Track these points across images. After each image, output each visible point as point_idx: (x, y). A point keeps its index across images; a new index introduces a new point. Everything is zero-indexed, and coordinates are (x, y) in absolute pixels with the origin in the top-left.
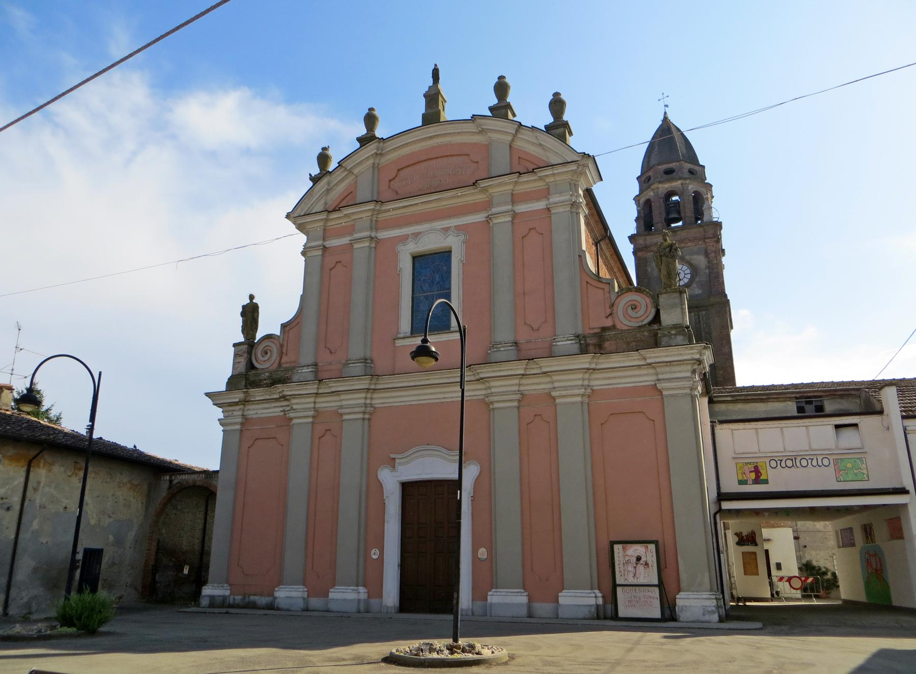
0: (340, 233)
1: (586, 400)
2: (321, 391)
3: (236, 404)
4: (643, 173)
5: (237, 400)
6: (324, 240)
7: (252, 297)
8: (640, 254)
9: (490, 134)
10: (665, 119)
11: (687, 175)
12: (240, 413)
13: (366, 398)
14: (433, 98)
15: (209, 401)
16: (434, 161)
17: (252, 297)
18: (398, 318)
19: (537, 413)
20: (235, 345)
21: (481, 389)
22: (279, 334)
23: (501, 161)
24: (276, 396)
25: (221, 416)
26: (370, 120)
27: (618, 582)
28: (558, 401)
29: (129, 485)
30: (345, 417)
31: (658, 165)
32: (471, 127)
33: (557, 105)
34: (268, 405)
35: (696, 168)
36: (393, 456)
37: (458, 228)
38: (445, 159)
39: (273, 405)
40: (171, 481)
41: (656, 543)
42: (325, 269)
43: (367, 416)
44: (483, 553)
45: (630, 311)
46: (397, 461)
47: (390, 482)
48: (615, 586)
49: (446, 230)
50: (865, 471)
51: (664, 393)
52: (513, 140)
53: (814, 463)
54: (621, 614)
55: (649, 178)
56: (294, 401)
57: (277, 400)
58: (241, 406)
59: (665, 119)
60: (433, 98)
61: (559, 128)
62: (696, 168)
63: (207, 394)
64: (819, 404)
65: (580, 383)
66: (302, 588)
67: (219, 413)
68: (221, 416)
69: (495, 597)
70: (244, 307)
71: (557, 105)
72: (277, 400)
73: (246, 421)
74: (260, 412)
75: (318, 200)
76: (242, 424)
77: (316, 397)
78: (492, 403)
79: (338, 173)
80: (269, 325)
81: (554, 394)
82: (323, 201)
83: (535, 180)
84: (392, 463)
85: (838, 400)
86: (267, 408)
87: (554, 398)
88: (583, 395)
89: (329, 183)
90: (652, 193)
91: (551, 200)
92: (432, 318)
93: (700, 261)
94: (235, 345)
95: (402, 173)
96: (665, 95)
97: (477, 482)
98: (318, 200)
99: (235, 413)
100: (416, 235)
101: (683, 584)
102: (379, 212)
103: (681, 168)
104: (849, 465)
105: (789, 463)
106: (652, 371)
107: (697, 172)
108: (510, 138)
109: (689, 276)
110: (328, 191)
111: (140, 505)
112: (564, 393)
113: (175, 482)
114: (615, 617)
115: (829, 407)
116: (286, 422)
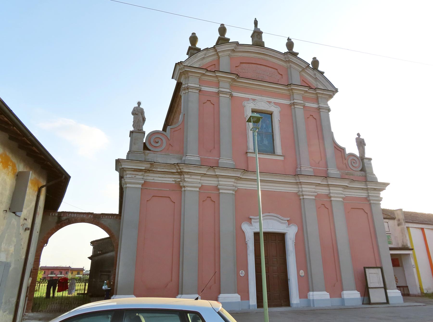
0: (210, 84)
2: (208, 173)
3: (141, 170)
5: (144, 168)
7: (139, 104)
9: (291, 64)
17: (139, 104)
18: (246, 142)
19: (325, 204)
21: (295, 188)
26: (222, 30)
30: (221, 191)
32: (282, 57)
34: (163, 176)
36: (251, 217)
37: (275, 103)
39: (167, 176)
43: (234, 193)
44: (302, 273)
46: (253, 220)
49: (270, 102)
56: (186, 176)
57: (173, 173)
72: (173, 173)
74: (155, 178)
75: (197, 61)
76: (143, 185)
78: (303, 195)
79: (211, 51)
83: (313, 93)
84: (249, 220)
86: (163, 177)
99: (137, 177)
100: (254, 100)
106: (366, 192)
112: (336, 195)
114: (369, 303)
116: (179, 187)
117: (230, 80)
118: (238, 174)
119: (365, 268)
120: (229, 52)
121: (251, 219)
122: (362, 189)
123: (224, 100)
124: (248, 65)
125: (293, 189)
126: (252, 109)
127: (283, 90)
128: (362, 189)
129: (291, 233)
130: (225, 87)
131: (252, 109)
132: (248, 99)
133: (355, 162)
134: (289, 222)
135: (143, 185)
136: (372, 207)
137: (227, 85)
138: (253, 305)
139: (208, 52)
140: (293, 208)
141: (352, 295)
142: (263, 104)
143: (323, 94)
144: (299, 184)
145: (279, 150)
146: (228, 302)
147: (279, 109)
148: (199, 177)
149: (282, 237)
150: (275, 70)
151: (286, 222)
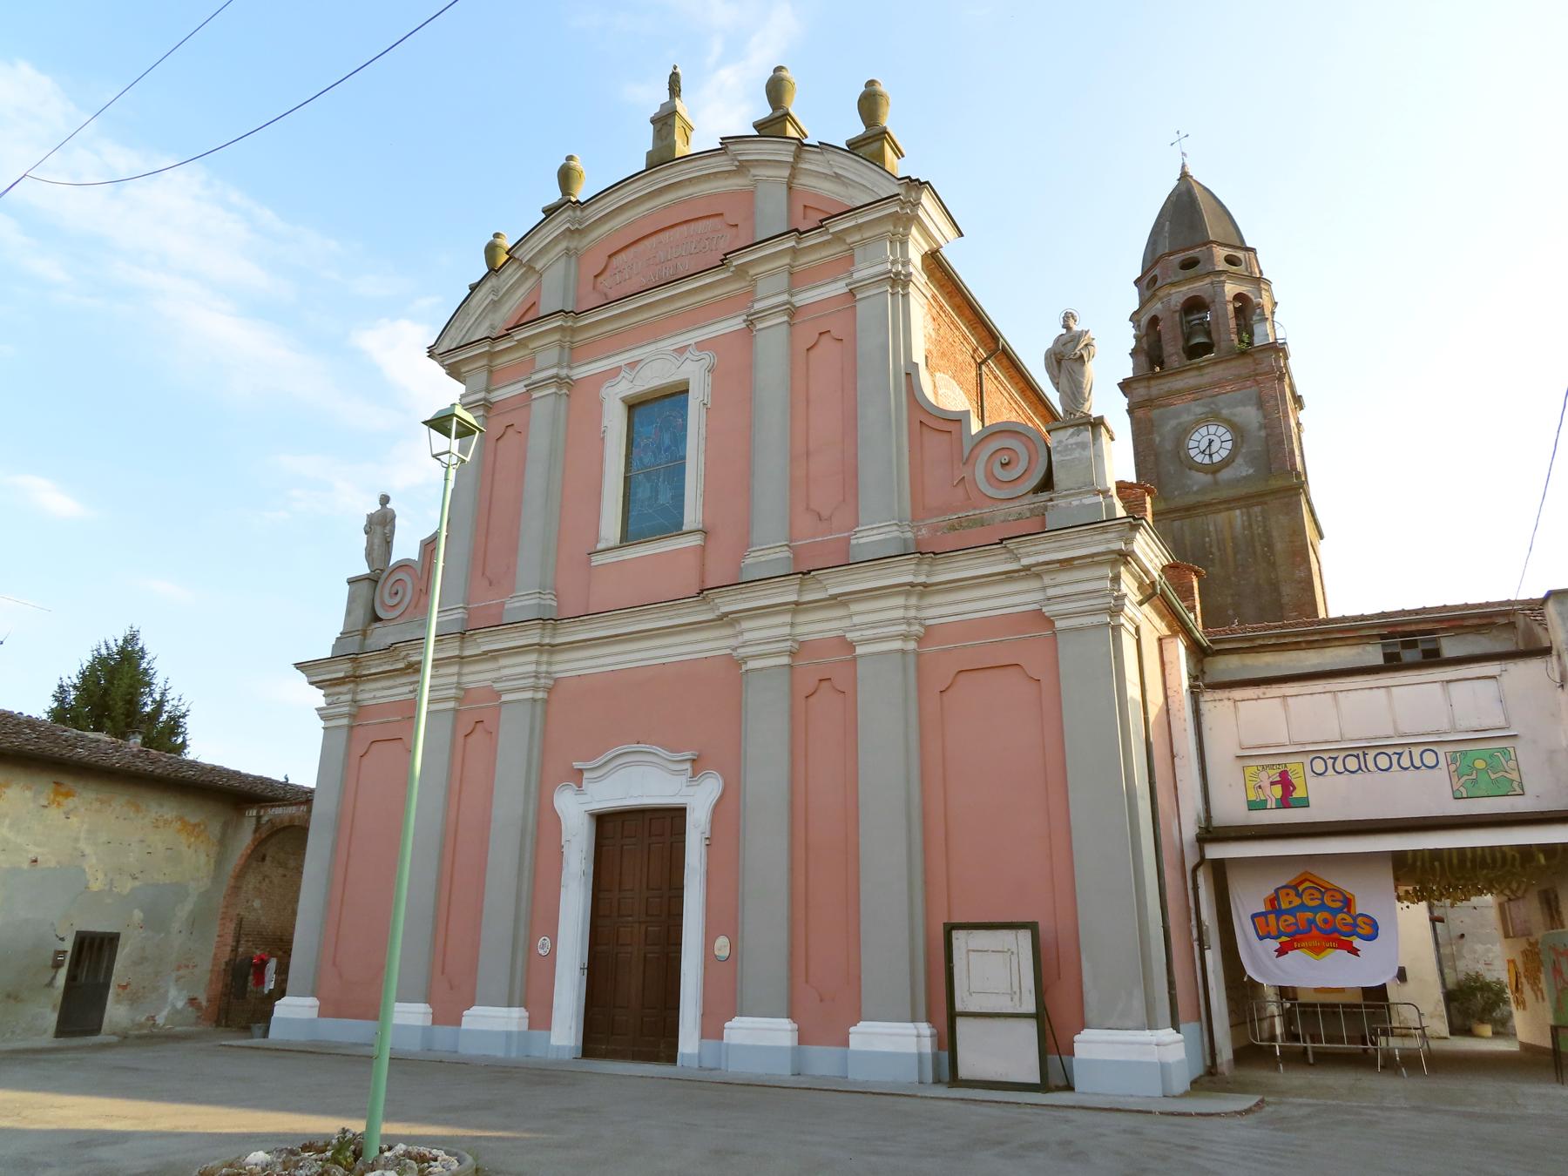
1: (912, 645)
2: (467, 653)
4: (1144, 274)
5: (341, 675)
6: (488, 391)
7: (385, 500)
8: (1139, 413)
9: (753, 171)
10: (1184, 176)
11: (1221, 265)
12: (349, 697)
13: (538, 663)
14: (665, 121)
15: (301, 678)
16: (666, 234)
19: (823, 678)
20: (351, 582)
22: (416, 557)
23: (773, 213)
24: (401, 665)
25: (322, 702)
26: (566, 176)
27: (959, 1007)
28: (860, 650)
29: (178, 825)
30: (505, 698)
31: (1170, 254)
32: (722, 164)
33: (870, 103)
35: (1240, 254)
36: (578, 765)
37: (700, 346)
38: (685, 227)
40: (259, 818)
41: (1032, 927)
42: (486, 435)
43: (540, 695)
44: (722, 946)
45: (999, 472)
46: (586, 775)
47: (574, 811)
48: (953, 1015)
49: (681, 351)
50: (1515, 776)
51: (1059, 624)
52: (792, 176)
53: (1405, 762)
54: (964, 1072)
55: (1154, 280)
58: (351, 686)
59: (1184, 176)
60: (665, 121)
61: (871, 144)
62: (1240, 254)
63: (299, 666)
64: (1430, 646)
65: (900, 613)
66: (423, 1008)
67: (318, 697)
68: (322, 702)
69: (743, 1030)
70: (370, 517)
71: (870, 103)
73: (358, 713)
74: (379, 694)
76: (351, 716)
77: (461, 664)
78: (744, 660)
79: (510, 271)
80: (405, 547)
81: (849, 636)
82: (487, 324)
83: (823, 244)
85: (1470, 637)
87: (851, 646)
88: (905, 637)
89: (495, 291)
90: (1159, 305)
91: (856, 276)
92: (651, 513)
93: (1249, 415)
94: (351, 582)
95: (616, 261)
96: (1182, 134)
97: (717, 809)
98: (478, 323)
99: (343, 698)
100: (632, 365)
101: (1091, 1014)
102: (574, 331)
103: (1211, 256)
104: (1480, 764)
105: (1352, 764)
107: (1240, 255)
108: (786, 173)
109: (1229, 445)
110: (496, 304)
111: (203, 859)
112: (869, 633)
113: (265, 819)
114: (955, 1080)
115: (1449, 648)
117: (557, 337)
118: (533, 637)
119: (950, 928)
120: (564, 245)
121: (581, 771)
122: (1009, 576)
123: (544, 405)
124: (632, 250)
125: (711, 644)
126: (624, 400)
127: (716, 285)
128: (1009, 576)
129: (700, 802)
130: (547, 362)
131: (624, 400)
132: (615, 372)
133: (1005, 459)
134: (698, 766)
135: (351, 716)
136: (1060, 645)
137: (553, 355)
138: (558, 1048)
139: (503, 277)
140: (698, 714)
141: (891, 1041)
142: (655, 367)
143: (859, 227)
144: (726, 620)
145: (692, 515)
146: (483, 1032)
147: (708, 358)
148: (455, 669)
149: (675, 817)
150: (716, 220)
151: (688, 766)
